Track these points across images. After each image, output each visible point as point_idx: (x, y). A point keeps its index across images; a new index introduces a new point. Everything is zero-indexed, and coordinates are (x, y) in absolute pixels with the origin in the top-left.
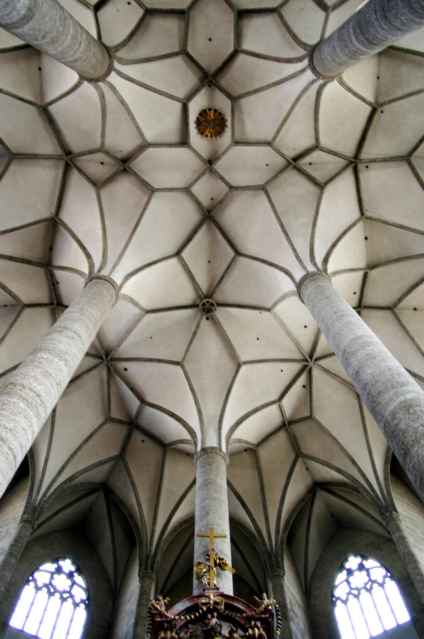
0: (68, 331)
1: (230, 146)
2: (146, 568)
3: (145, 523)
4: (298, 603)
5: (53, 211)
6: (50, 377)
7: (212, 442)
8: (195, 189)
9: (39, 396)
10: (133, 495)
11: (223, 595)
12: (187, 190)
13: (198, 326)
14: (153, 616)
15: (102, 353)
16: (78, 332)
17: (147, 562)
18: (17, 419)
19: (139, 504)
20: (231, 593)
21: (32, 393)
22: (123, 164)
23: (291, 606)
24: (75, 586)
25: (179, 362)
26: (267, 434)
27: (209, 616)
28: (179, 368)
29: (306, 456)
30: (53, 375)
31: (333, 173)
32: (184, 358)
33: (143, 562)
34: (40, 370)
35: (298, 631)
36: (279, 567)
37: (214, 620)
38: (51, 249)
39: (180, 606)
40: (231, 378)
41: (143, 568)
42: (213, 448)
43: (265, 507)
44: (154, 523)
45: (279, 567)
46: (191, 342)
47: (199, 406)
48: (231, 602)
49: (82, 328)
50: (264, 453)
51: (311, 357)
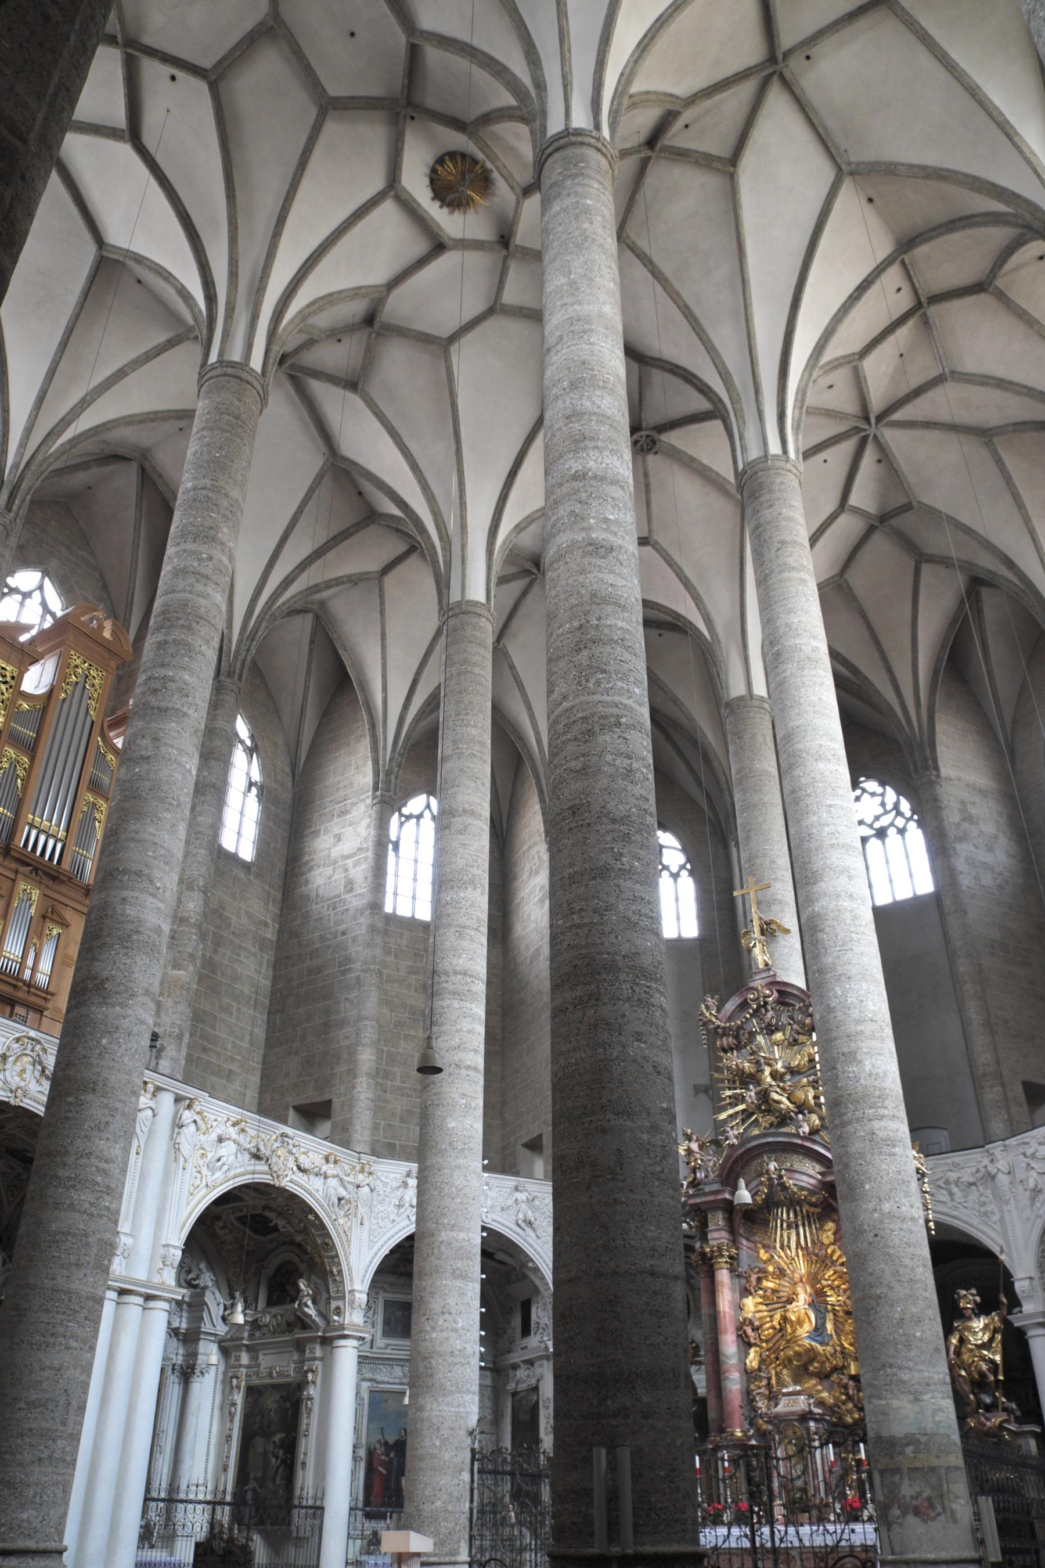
0: (457, 819)
1: (518, 203)
3: (716, 754)
4: (983, 793)
5: (324, 449)
6: (467, 931)
8: (509, 297)
9: (465, 973)
11: (773, 983)
12: (494, 309)
15: (529, 566)
16: (467, 806)
18: (458, 1027)
21: (459, 977)
22: (371, 329)
24: (664, 850)
26: (850, 549)
27: (763, 1010)
29: (933, 559)
30: (467, 923)
31: (740, 119)
32: (650, 530)
34: (452, 930)
35: (976, 847)
36: (926, 768)
37: (770, 1014)
38: (360, 493)
39: (731, 1006)
42: (741, 698)
47: (705, 608)
48: (783, 989)
49: (470, 791)
50: (857, 579)
51: (867, 419)
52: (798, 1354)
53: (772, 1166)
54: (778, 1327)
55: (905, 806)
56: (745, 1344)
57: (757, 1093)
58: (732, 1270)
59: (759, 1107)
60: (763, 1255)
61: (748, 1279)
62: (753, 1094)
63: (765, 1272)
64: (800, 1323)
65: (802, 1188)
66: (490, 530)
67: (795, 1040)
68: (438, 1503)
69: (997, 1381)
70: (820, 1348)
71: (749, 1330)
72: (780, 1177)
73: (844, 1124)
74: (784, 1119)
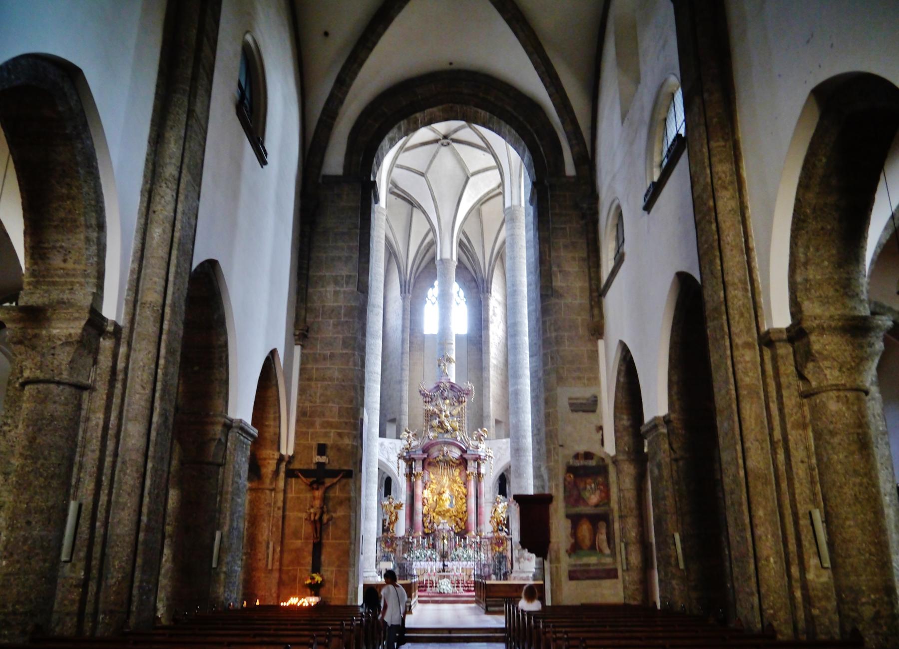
2: (405, 293)
4: (499, 303)
7: (447, 256)
10: (391, 234)
11: (450, 382)
13: (437, 152)
14: (420, 391)
17: (405, 286)
19: (396, 242)
20: (454, 382)
23: (494, 311)
25: (423, 173)
28: (423, 178)
33: (403, 287)
36: (487, 292)
37: (446, 393)
40: (462, 187)
41: (403, 292)
42: (447, 260)
43: (483, 247)
44: (407, 257)
45: (487, 292)
46: (431, 162)
52: (444, 511)
53: (445, 449)
54: (435, 500)
55: (462, 293)
56: (424, 505)
57: (439, 422)
58: (422, 481)
59: (438, 426)
60: (432, 476)
61: (426, 484)
62: (437, 421)
63: (432, 482)
64: (446, 501)
65: (453, 457)
66: (388, 172)
67: (454, 404)
68: (369, 554)
69: (504, 523)
70: (451, 509)
71: (426, 501)
72: (447, 453)
73: (519, 456)
74: (447, 431)
